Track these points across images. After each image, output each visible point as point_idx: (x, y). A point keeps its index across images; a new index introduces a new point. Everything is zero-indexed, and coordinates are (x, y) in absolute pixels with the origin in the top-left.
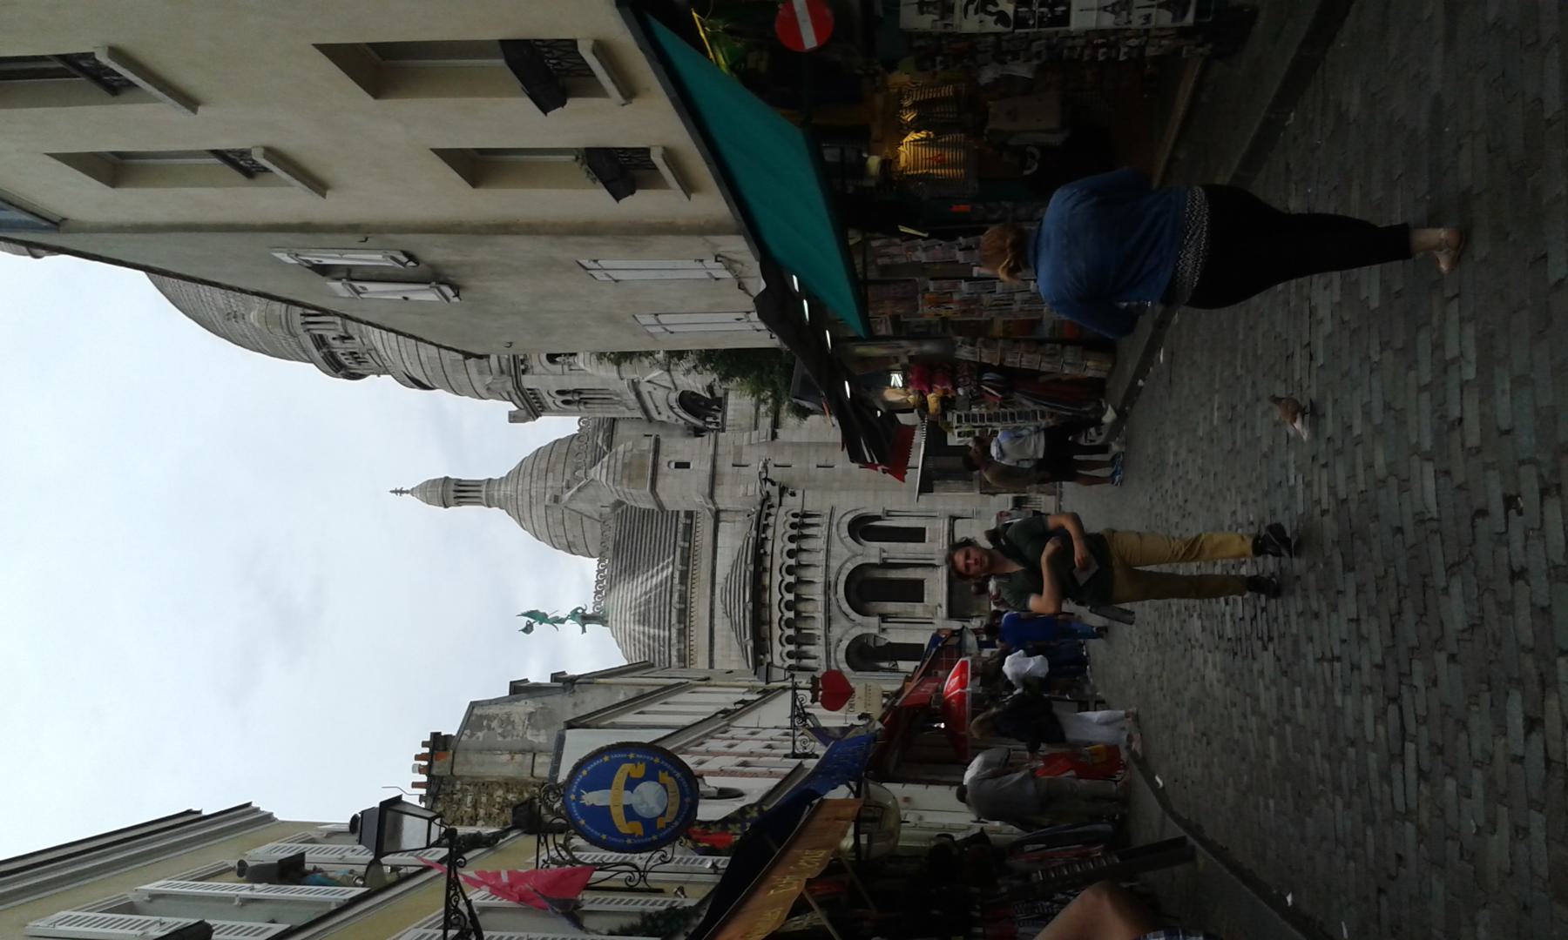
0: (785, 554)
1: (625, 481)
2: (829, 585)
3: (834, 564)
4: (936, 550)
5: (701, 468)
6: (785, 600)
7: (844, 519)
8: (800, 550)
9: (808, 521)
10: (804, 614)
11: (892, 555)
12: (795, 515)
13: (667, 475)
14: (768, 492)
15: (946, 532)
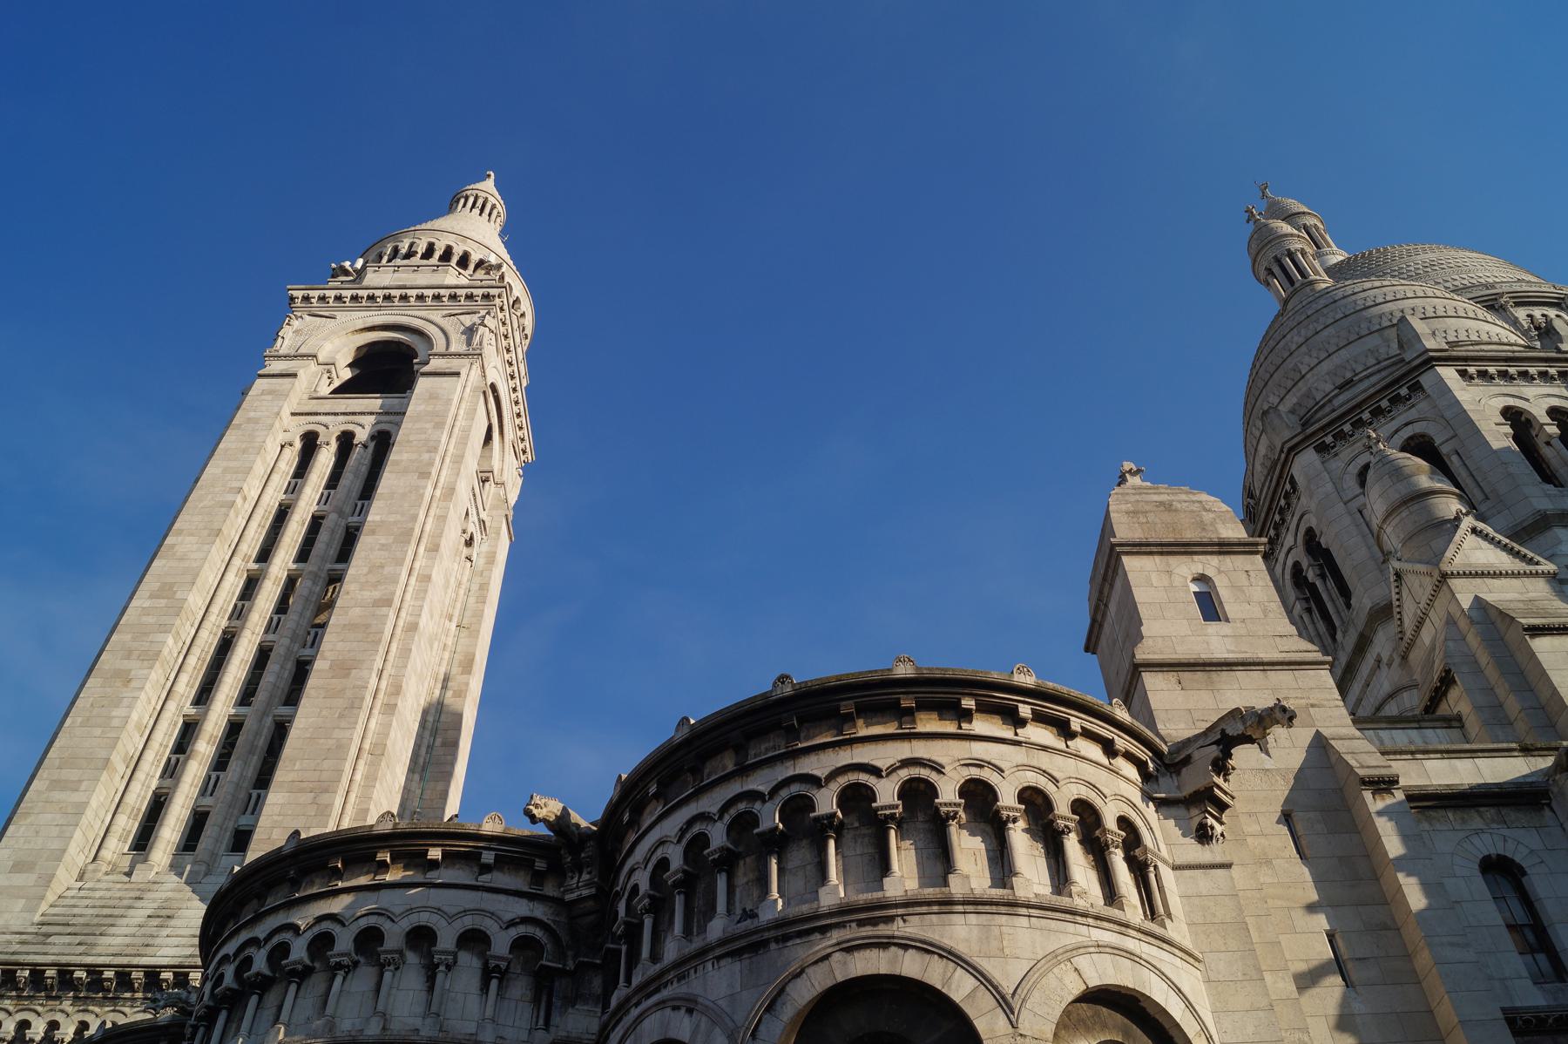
0: (975, 772)
2: (874, 922)
5: (1216, 642)
9: (1118, 860)
12: (1123, 822)
14: (1187, 761)
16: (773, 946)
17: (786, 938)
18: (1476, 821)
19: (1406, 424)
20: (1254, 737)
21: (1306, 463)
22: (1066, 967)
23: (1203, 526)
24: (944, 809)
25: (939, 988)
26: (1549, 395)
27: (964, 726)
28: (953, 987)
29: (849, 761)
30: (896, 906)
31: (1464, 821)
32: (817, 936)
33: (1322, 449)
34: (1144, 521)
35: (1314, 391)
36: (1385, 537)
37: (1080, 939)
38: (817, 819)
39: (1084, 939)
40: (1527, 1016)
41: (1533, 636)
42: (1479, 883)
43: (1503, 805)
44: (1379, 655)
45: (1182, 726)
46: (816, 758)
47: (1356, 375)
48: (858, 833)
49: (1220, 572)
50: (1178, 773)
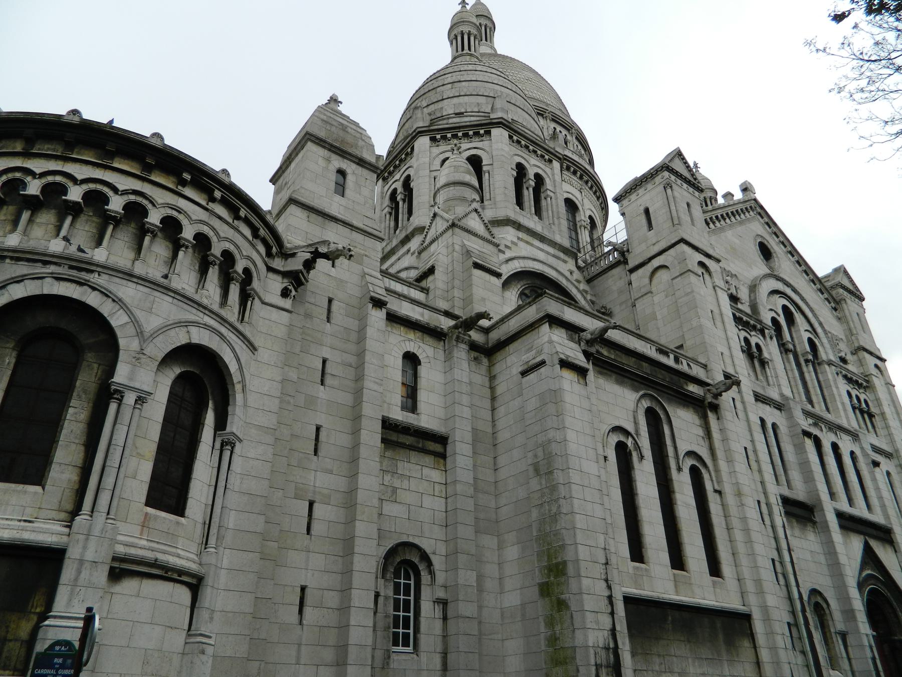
0: (175, 214)
1: (325, 118)
3: (128, 291)
4: (122, 527)
5: (335, 206)
6: (70, 184)
7: (228, 350)
8: (177, 245)
10: (26, 215)
11: (126, 412)
13: (328, 160)
14: (293, 255)
15: (161, 557)
16: (8, 261)
17: (18, 259)
18: (411, 335)
19: (475, 148)
20: (330, 257)
21: (423, 143)
22: (185, 329)
23: (356, 146)
24: (147, 226)
25: (106, 315)
26: (539, 167)
27: (180, 187)
28: (115, 318)
29: (100, 177)
30: (97, 265)
31: (406, 333)
32: (40, 265)
33: (433, 139)
34: (329, 129)
35: (444, 110)
36: (438, 195)
37: (197, 318)
38: (66, 201)
39: (199, 319)
40: (391, 422)
41: (475, 267)
42: (399, 362)
43: (427, 333)
44: (410, 248)
45: (300, 238)
46: (80, 166)
47: (466, 112)
48: (91, 218)
49: (354, 173)
50: (286, 259)
